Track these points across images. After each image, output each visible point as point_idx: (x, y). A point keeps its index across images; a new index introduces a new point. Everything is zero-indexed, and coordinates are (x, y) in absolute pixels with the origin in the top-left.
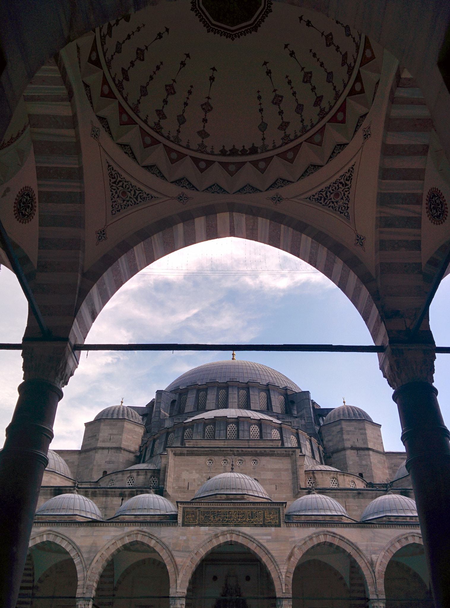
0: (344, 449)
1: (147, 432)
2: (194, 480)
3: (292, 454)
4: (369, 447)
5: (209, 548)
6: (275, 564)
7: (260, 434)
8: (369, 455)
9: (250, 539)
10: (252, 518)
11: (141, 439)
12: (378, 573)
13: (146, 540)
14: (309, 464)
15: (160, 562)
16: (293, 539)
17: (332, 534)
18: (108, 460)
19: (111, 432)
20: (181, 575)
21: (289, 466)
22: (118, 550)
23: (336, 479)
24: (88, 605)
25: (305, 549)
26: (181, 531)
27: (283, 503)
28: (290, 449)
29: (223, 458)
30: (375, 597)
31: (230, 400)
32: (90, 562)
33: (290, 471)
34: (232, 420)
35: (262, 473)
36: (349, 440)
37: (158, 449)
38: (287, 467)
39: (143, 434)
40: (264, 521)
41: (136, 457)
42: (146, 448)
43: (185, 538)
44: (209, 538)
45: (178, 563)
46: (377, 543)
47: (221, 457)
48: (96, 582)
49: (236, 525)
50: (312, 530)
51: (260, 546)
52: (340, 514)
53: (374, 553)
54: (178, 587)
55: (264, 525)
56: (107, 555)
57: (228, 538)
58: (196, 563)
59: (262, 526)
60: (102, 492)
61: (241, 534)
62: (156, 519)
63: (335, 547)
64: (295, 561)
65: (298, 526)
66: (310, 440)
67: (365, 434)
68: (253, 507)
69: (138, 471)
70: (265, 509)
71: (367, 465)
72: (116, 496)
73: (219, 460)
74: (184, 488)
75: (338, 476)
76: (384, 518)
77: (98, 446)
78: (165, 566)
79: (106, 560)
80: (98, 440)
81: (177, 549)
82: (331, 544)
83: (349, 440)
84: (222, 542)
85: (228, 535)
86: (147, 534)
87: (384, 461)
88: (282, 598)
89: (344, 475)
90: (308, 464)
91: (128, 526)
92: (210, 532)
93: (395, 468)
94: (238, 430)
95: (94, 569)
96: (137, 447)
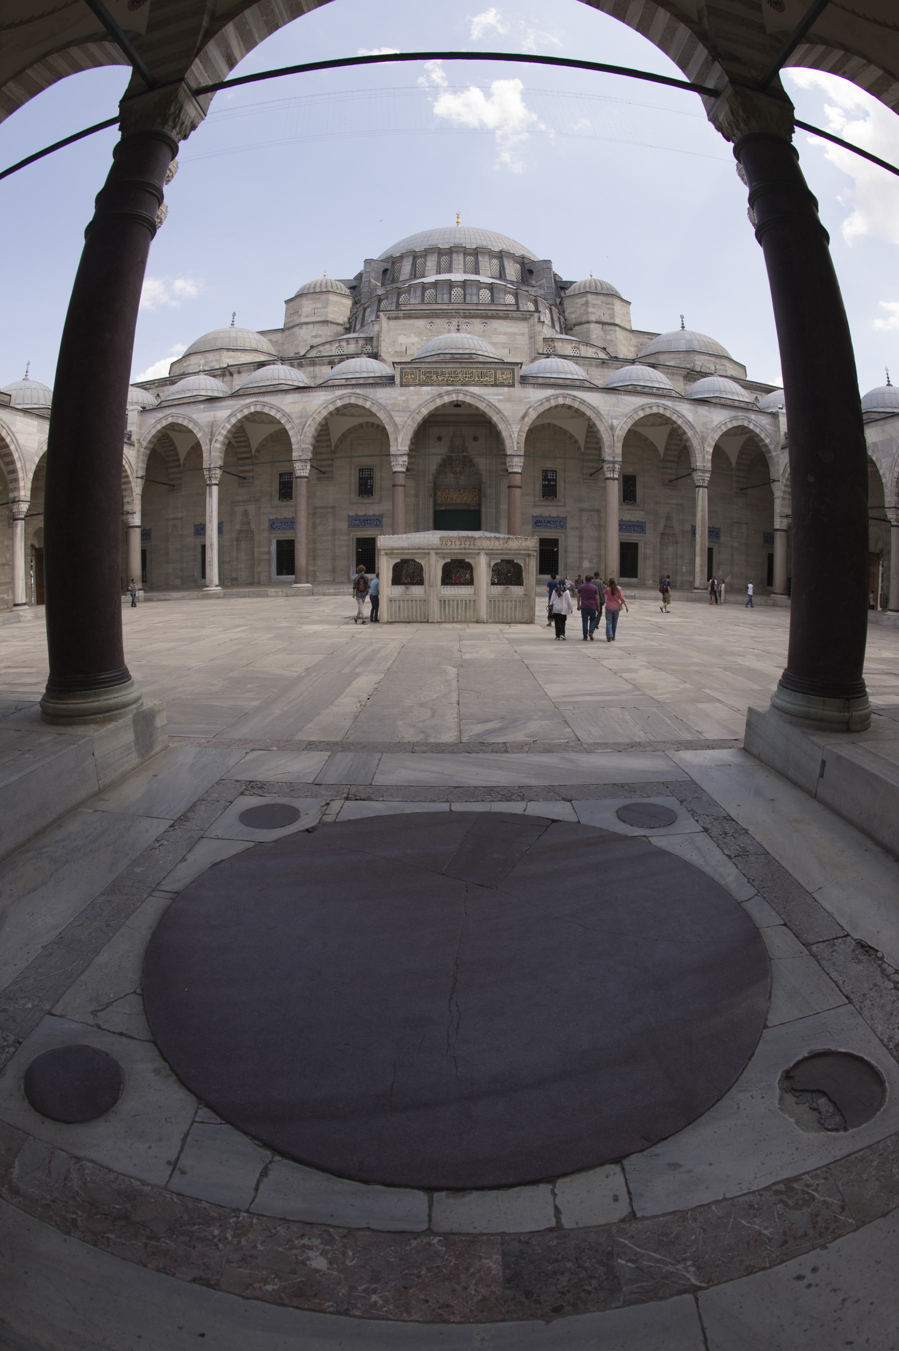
0: (588, 322)
1: (355, 303)
2: (413, 344)
3: (530, 318)
4: (616, 322)
5: (432, 407)
6: (507, 423)
7: (491, 298)
8: (615, 331)
9: (479, 398)
10: (482, 378)
11: (349, 311)
12: (618, 437)
13: (360, 402)
14: (547, 332)
15: (378, 426)
16: (528, 400)
17: (572, 397)
18: (314, 334)
19: (314, 306)
20: (402, 435)
21: (526, 331)
22: (331, 414)
23: (578, 348)
25: (541, 410)
26: (399, 391)
27: (518, 364)
28: (527, 313)
29: (447, 321)
30: (611, 459)
31: (455, 266)
32: (302, 427)
33: (527, 336)
34: (459, 284)
35: (493, 336)
36: (594, 313)
37: (370, 316)
38: (522, 332)
39: (351, 305)
40: (495, 380)
41: (346, 329)
42: (356, 318)
43: (404, 398)
44: (432, 398)
45: (397, 422)
46: (620, 409)
47: (444, 320)
48: (311, 445)
49: (462, 385)
50: (550, 392)
51: (491, 405)
52: (582, 378)
53: (616, 419)
54: (399, 445)
55: (495, 385)
56: (319, 419)
57: (454, 397)
58: (417, 423)
59: (492, 386)
60: (308, 362)
61: (468, 394)
62: (371, 381)
63: (574, 410)
64: (529, 421)
65: (534, 388)
66: (551, 310)
67: (613, 309)
69: (348, 340)
70: (498, 369)
71: (612, 341)
72: (324, 365)
73: (440, 323)
74: (401, 352)
75: (580, 346)
76: (630, 387)
77: (302, 321)
78: (384, 429)
79: (319, 424)
80: (301, 315)
81: (396, 409)
82: (570, 407)
83: (594, 313)
84: (446, 401)
85: (454, 395)
86: (360, 396)
87: (631, 338)
88: (514, 455)
89: (587, 346)
90: (546, 332)
91: (339, 389)
92: (433, 392)
93: (641, 347)
94: (465, 294)
95: (307, 433)
96: (346, 319)
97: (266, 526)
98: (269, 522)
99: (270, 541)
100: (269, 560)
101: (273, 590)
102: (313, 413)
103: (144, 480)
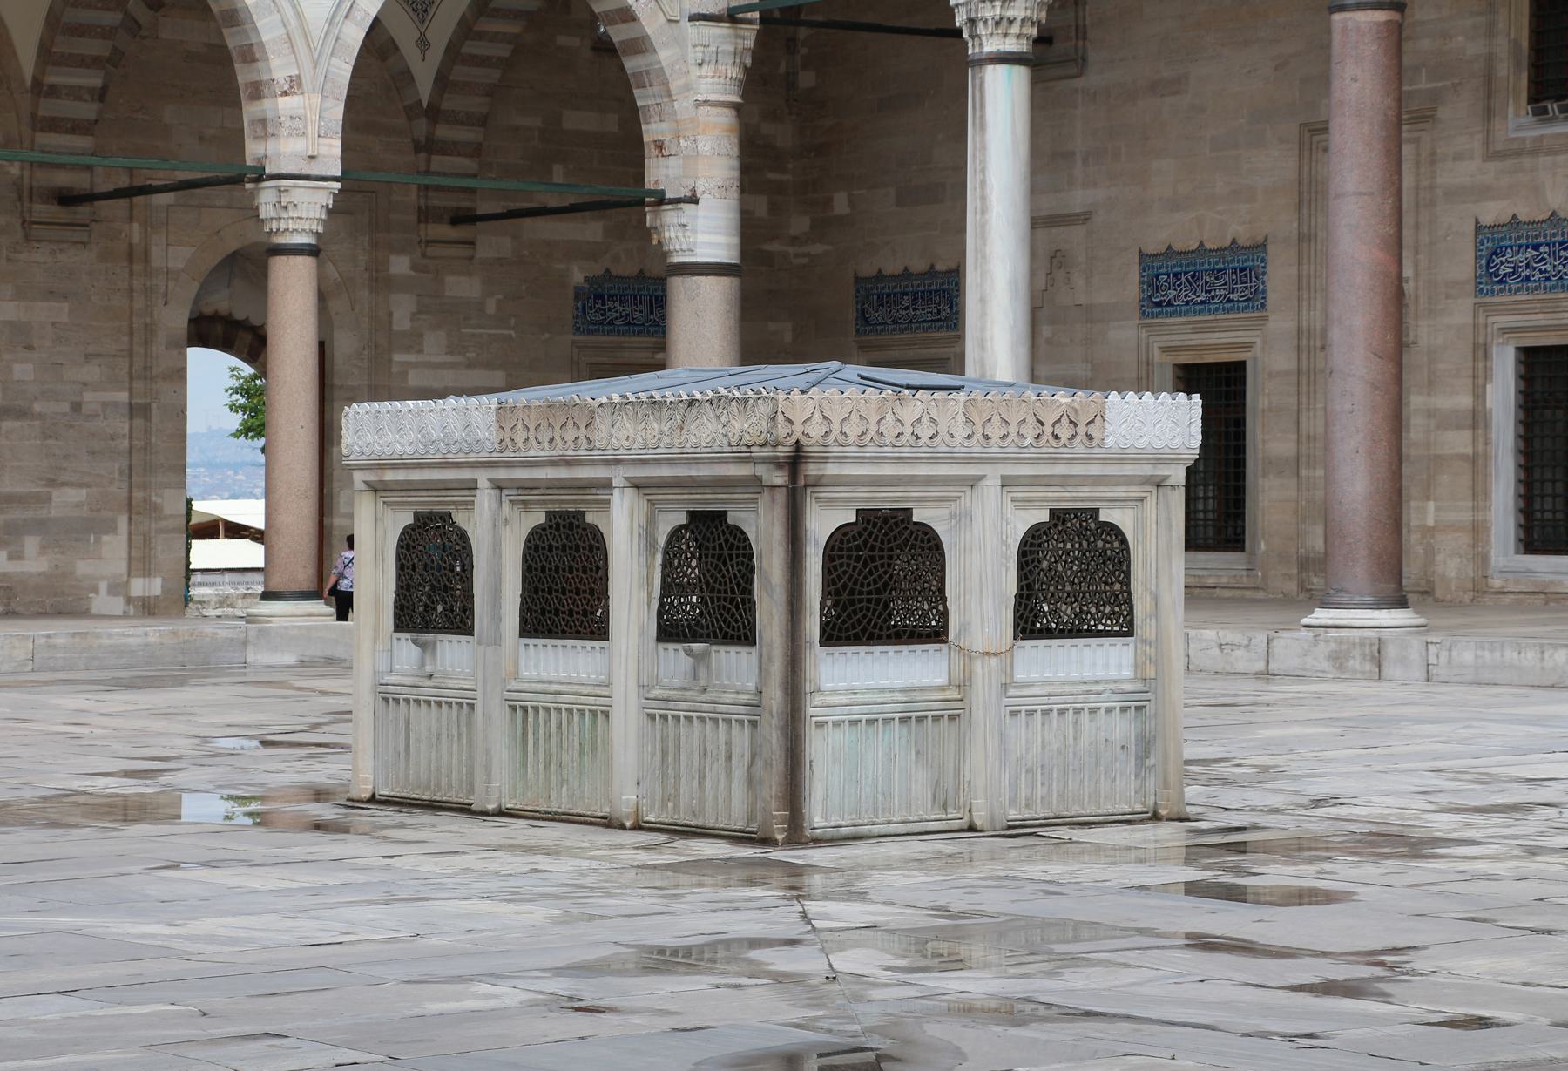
97: (1462, 264)
98: (1478, 245)
99: (1481, 352)
100: (1477, 464)
101: (1210, 634)
103: (749, 34)
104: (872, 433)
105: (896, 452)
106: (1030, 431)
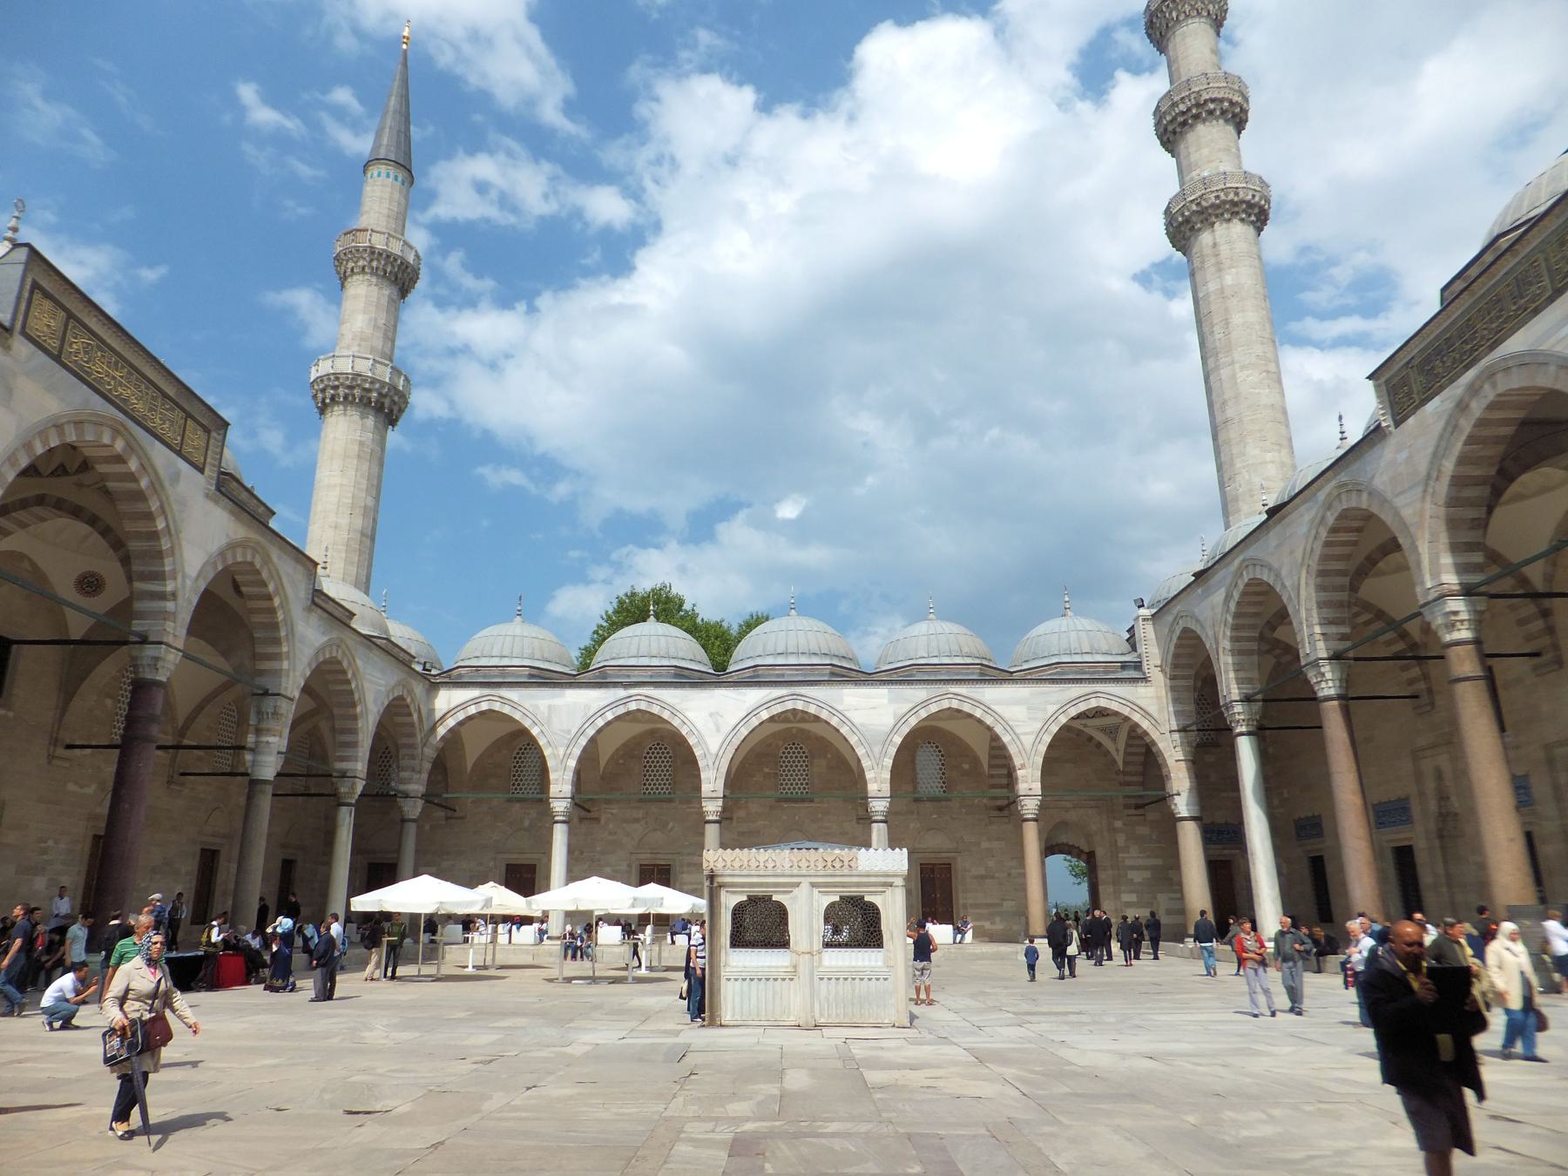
24: (1323, 675)
43: (1404, 455)
68: (1517, 260)
102: (1303, 559)
104: (745, 865)
105: (757, 873)
106: (820, 865)
